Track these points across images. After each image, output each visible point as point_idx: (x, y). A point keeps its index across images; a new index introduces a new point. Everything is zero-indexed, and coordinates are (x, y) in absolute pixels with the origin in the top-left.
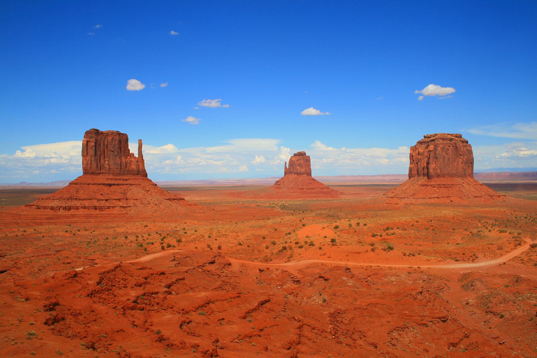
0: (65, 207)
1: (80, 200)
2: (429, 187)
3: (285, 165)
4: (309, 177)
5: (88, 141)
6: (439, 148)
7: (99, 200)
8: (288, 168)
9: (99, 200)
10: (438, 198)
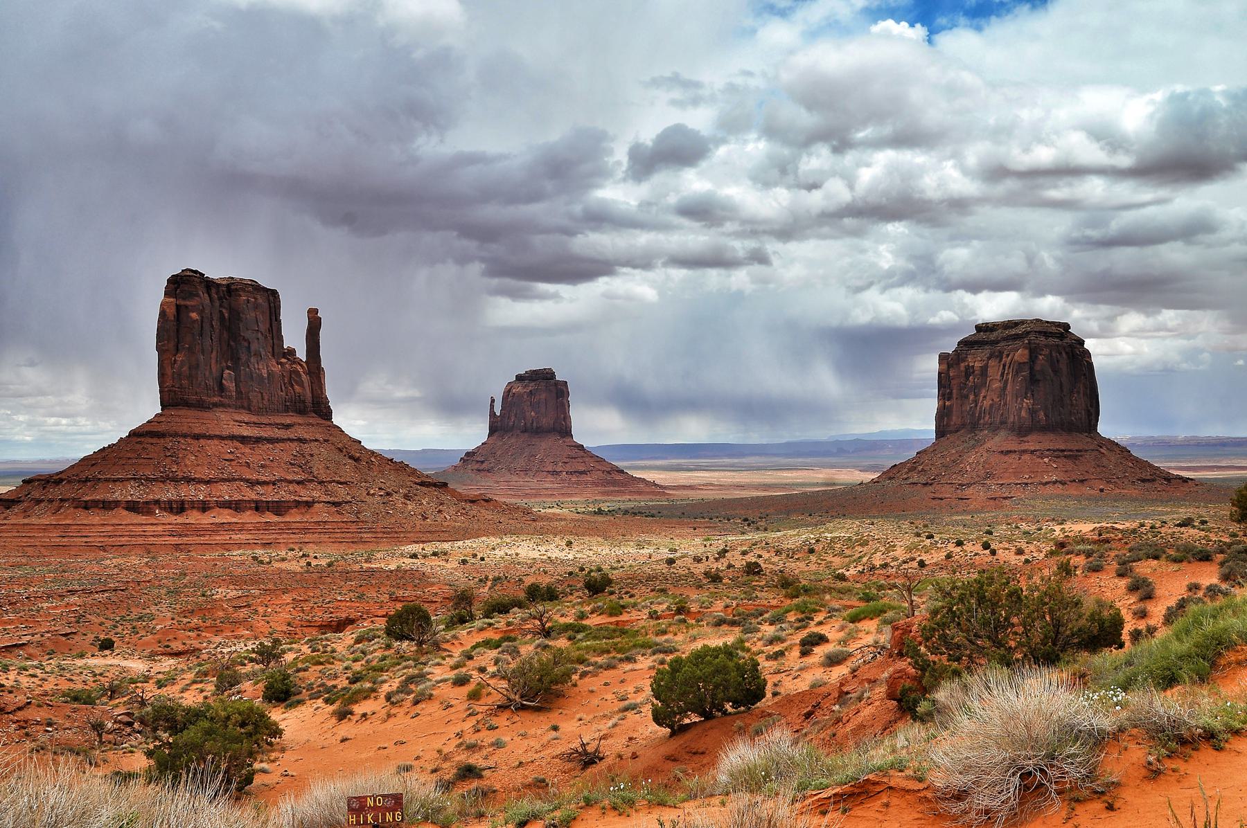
0: (170, 502)
1: (201, 481)
2: (1026, 457)
3: (492, 406)
4: (567, 440)
5: (178, 307)
6: (1041, 357)
7: (253, 484)
8: (498, 414)
9: (253, 484)
10: (1063, 483)
